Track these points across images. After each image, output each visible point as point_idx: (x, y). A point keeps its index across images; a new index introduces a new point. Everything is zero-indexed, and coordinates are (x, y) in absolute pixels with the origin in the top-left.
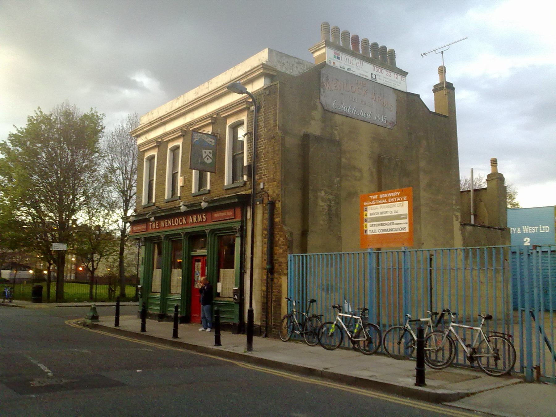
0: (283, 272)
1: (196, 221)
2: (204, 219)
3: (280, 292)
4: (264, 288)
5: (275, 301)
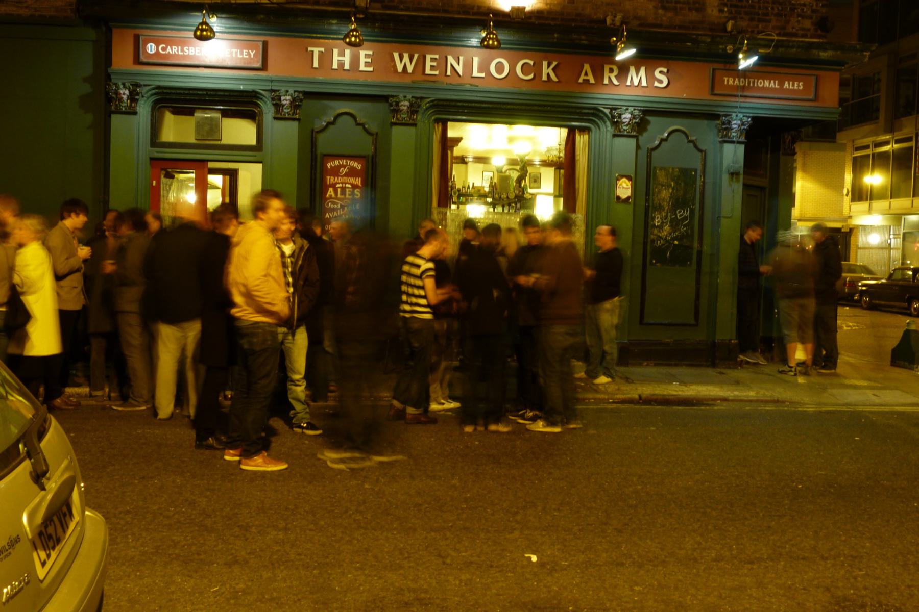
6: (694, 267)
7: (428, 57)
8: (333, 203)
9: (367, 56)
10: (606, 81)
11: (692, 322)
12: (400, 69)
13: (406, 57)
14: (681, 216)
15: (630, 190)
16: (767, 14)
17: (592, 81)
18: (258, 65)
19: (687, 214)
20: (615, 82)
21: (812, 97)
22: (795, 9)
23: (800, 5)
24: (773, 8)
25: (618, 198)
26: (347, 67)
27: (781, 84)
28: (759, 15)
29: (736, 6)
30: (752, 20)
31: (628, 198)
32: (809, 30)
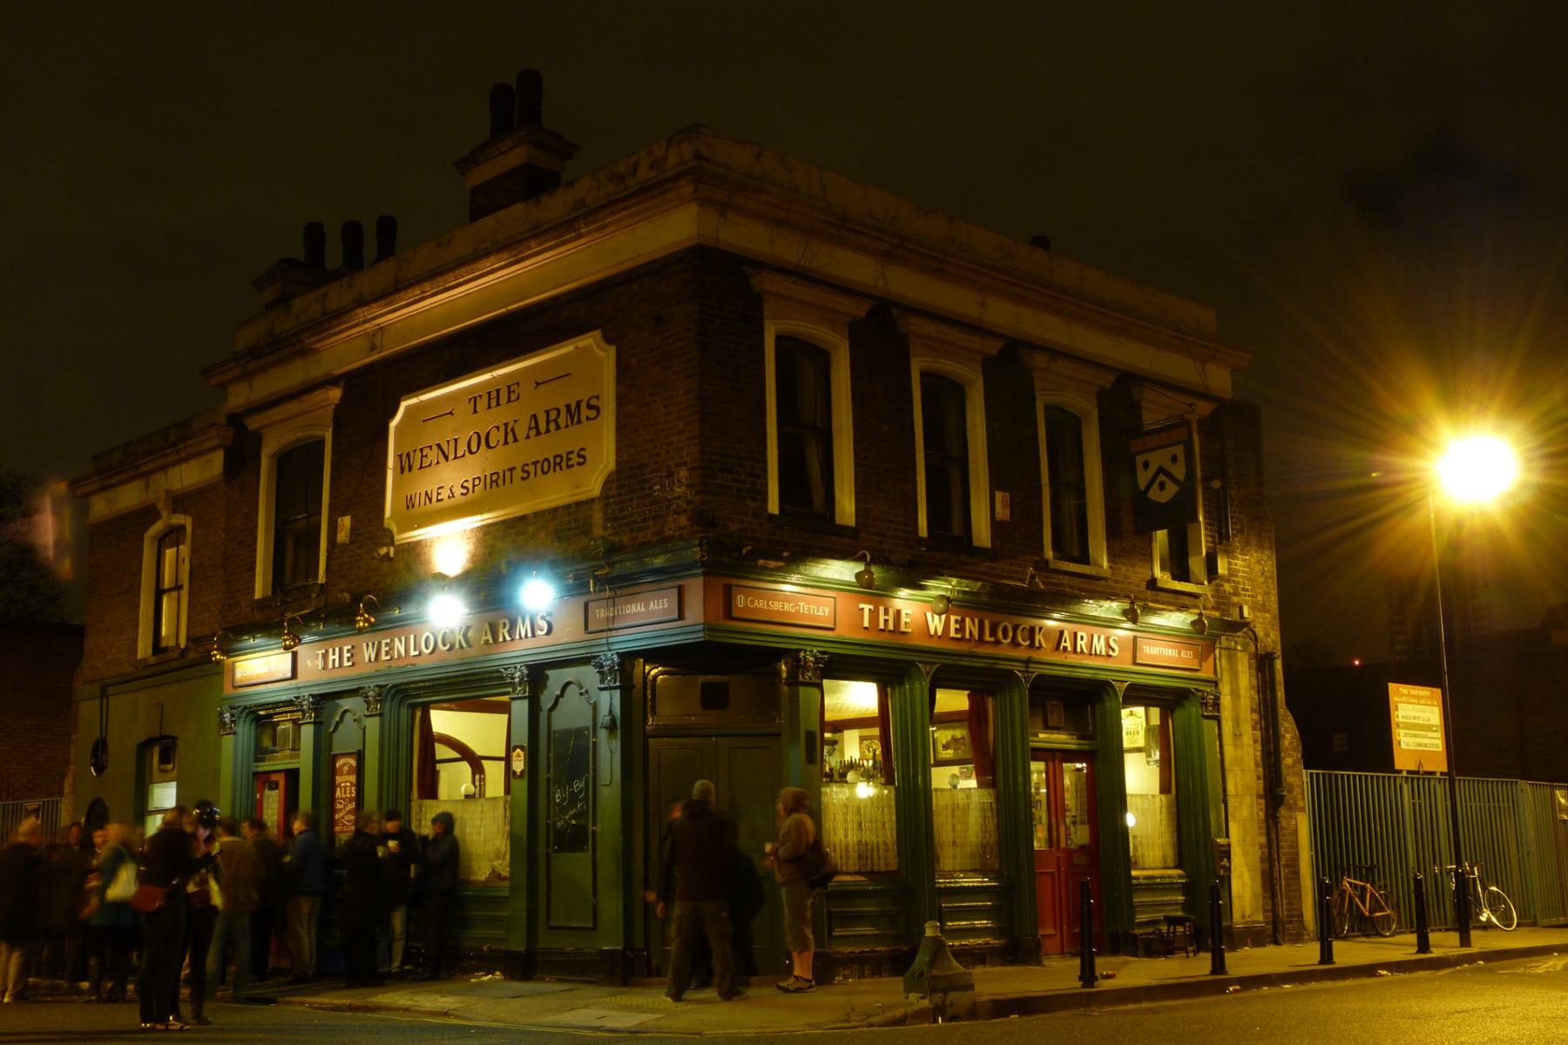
0: (1296, 804)
1: (1085, 651)
2: (1113, 650)
3: (1295, 846)
4: (1263, 840)
5: (1285, 866)
6: (590, 853)
7: (384, 642)
8: (341, 803)
9: (348, 651)
10: (501, 639)
11: (590, 925)
12: (367, 660)
13: (370, 644)
14: (577, 788)
15: (523, 762)
16: (644, 520)
17: (491, 641)
18: (289, 675)
19: (582, 785)
20: (508, 638)
21: (676, 616)
22: (671, 505)
23: (675, 498)
24: (650, 511)
25: (514, 772)
26: (337, 665)
27: (647, 606)
28: (637, 522)
29: (617, 519)
30: (632, 531)
31: (522, 772)
32: (684, 528)
